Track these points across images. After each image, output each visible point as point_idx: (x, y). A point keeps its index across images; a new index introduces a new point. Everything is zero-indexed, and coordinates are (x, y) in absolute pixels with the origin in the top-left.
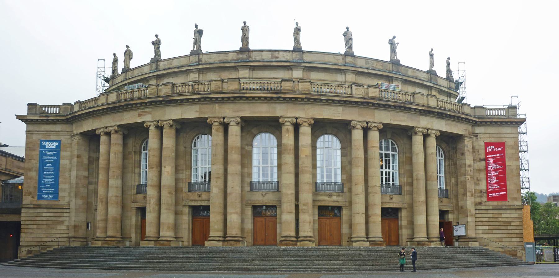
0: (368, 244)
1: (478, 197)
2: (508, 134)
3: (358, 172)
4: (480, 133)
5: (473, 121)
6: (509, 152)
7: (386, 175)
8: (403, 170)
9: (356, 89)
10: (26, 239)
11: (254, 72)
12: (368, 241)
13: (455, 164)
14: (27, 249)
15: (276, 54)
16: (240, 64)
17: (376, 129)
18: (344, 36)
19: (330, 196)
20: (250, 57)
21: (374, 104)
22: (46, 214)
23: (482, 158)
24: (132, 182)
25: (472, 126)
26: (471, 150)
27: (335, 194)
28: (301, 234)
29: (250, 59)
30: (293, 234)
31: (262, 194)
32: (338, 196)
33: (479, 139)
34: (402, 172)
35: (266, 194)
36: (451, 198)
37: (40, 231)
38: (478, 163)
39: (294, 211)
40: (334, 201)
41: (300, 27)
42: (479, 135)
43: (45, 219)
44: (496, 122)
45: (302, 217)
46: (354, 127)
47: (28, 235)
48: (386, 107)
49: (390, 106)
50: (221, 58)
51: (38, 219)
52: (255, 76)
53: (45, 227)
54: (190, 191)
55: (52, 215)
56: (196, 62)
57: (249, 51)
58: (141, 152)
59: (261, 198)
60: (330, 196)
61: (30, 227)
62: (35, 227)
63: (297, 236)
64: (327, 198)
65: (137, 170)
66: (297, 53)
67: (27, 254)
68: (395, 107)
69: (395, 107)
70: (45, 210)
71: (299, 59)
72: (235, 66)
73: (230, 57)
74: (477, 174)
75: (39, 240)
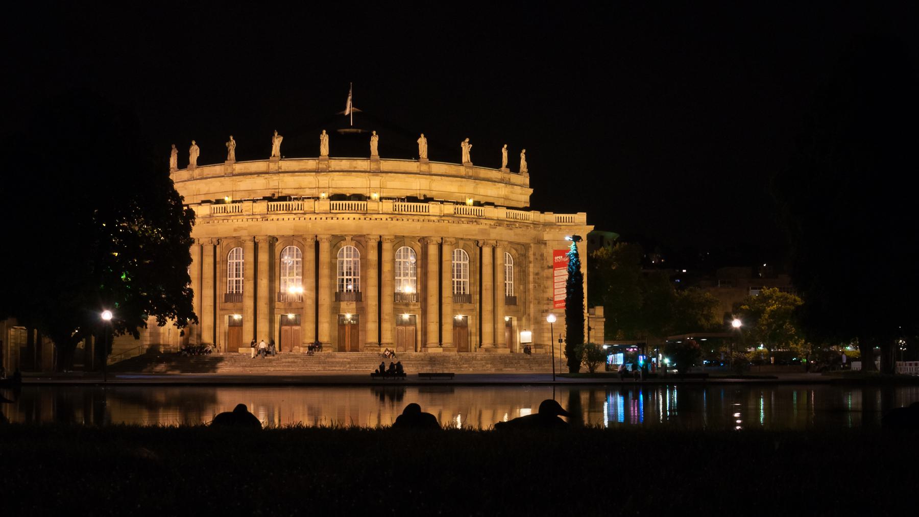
0: (440, 350)
1: (545, 304)
3: (433, 285)
4: (549, 241)
7: (457, 284)
8: (473, 279)
9: (433, 207)
12: (441, 347)
13: (524, 271)
23: (550, 266)
24: (222, 291)
28: (384, 341)
33: (548, 247)
34: (473, 282)
35: (350, 304)
36: (519, 305)
38: (546, 271)
39: (378, 321)
42: (547, 242)
54: (279, 301)
56: (276, 170)
58: (227, 261)
63: (380, 343)
65: (224, 279)
71: (377, 170)
74: (545, 282)
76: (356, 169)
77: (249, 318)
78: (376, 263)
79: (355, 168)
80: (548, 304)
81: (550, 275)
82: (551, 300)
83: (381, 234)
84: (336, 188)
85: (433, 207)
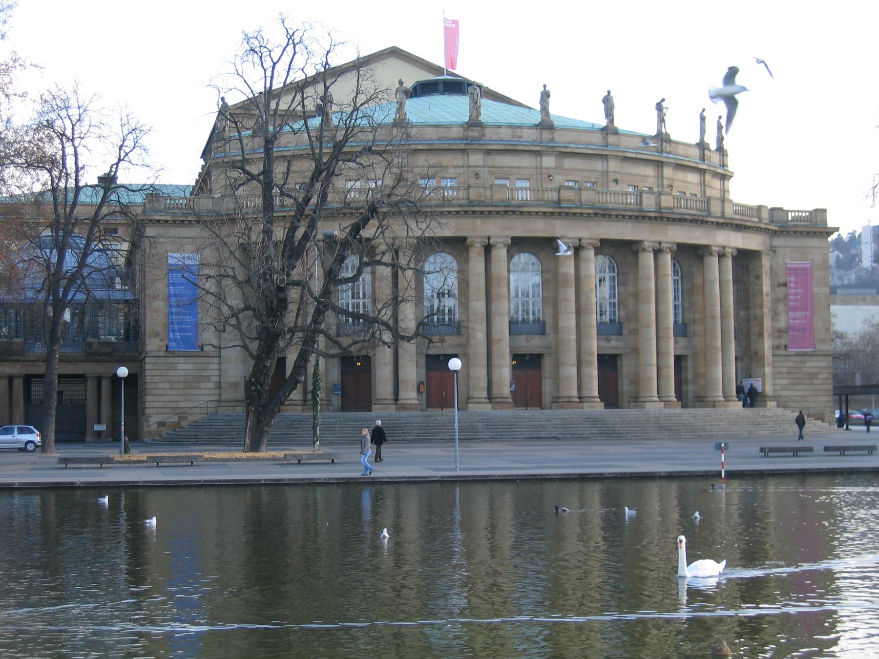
0: (662, 404)
2: (815, 247)
4: (779, 247)
5: (772, 230)
9: (648, 198)
10: (155, 404)
11: (489, 157)
12: (660, 401)
14: (158, 420)
15: (518, 132)
16: (473, 147)
17: (668, 250)
18: (604, 102)
19: (608, 340)
20: (484, 135)
21: (668, 219)
22: (184, 367)
25: (771, 237)
26: (769, 272)
27: (614, 337)
29: (484, 138)
30: (574, 393)
31: (527, 339)
32: (617, 340)
37: (176, 392)
38: (777, 290)
40: (614, 348)
41: (549, 91)
42: (778, 249)
43: (182, 373)
44: (801, 232)
46: (644, 250)
47: (158, 398)
48: (681, 220)
49: (686, 220)
50: (440, 135)
51: (172, 373)
52: (490, 164)
53: (182, 385)
55: (191, 367)
57: (481, 125)
59: (525, 344)
60: (608, 340)
61: (160, 385)
62: (167, 385)
64: (604, 344)
66: (548, 131)
67: (158, 427)
68: (691, 221)
69: (691, 221)
70: (181, 360)
72: (465, 150)
73: (456, 132)
75: (174, 405)
76: (520, 140)
77: (387, 360)
78: (573, 278)
79: (520, 137)
80: (780, 337)
81: (781, 296)
82: (783, 332)
83: (581, 236)
84: (493, 167)
85: (648, 198)
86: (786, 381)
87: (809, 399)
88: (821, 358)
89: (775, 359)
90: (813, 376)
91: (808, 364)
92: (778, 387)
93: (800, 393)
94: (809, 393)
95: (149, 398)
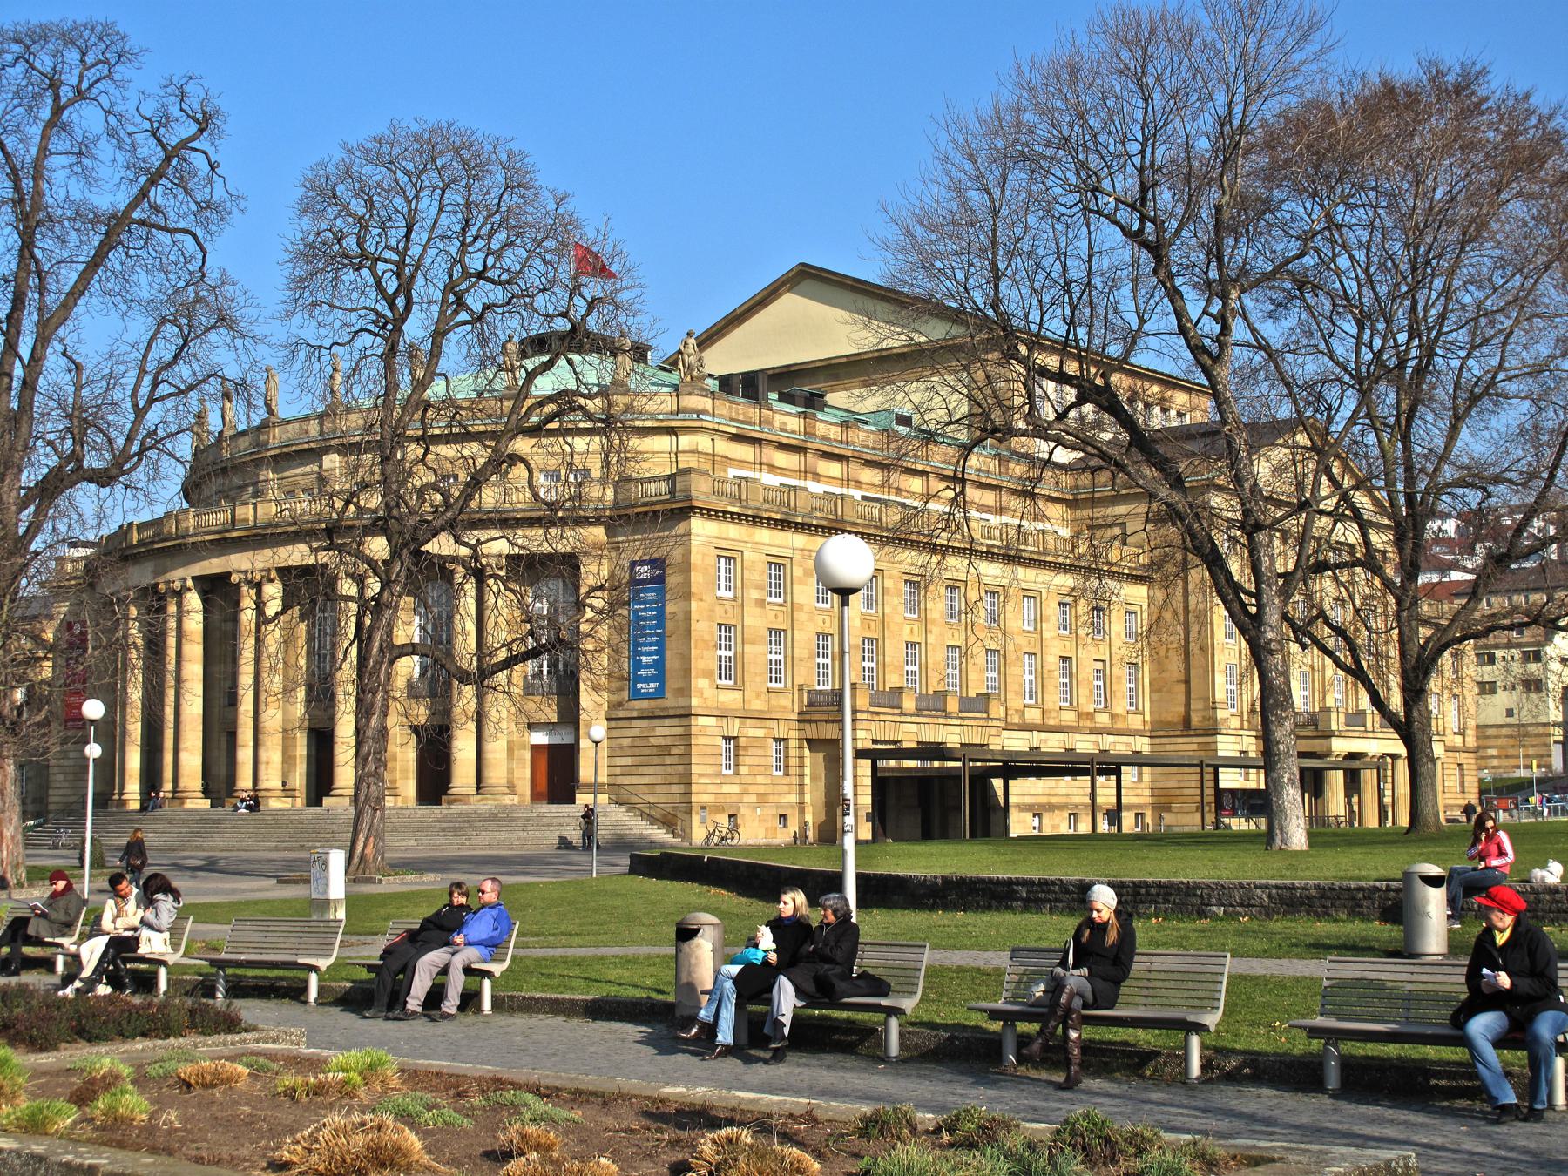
6: (673, 580)
45: (263, 755)
80: (621, 689)
86: (628, 761)
87: (658, 789)
88: (675, 721)
89: (613, 724)
90: (665, 750)
91: (659, 731)
92: (618, 771)
93: (646, 780)
94: (659, 779)
95: (51, 792)
